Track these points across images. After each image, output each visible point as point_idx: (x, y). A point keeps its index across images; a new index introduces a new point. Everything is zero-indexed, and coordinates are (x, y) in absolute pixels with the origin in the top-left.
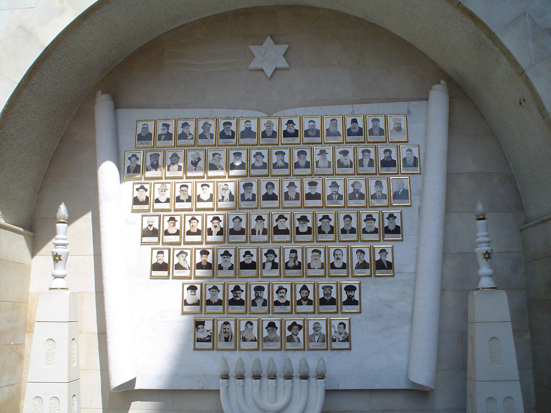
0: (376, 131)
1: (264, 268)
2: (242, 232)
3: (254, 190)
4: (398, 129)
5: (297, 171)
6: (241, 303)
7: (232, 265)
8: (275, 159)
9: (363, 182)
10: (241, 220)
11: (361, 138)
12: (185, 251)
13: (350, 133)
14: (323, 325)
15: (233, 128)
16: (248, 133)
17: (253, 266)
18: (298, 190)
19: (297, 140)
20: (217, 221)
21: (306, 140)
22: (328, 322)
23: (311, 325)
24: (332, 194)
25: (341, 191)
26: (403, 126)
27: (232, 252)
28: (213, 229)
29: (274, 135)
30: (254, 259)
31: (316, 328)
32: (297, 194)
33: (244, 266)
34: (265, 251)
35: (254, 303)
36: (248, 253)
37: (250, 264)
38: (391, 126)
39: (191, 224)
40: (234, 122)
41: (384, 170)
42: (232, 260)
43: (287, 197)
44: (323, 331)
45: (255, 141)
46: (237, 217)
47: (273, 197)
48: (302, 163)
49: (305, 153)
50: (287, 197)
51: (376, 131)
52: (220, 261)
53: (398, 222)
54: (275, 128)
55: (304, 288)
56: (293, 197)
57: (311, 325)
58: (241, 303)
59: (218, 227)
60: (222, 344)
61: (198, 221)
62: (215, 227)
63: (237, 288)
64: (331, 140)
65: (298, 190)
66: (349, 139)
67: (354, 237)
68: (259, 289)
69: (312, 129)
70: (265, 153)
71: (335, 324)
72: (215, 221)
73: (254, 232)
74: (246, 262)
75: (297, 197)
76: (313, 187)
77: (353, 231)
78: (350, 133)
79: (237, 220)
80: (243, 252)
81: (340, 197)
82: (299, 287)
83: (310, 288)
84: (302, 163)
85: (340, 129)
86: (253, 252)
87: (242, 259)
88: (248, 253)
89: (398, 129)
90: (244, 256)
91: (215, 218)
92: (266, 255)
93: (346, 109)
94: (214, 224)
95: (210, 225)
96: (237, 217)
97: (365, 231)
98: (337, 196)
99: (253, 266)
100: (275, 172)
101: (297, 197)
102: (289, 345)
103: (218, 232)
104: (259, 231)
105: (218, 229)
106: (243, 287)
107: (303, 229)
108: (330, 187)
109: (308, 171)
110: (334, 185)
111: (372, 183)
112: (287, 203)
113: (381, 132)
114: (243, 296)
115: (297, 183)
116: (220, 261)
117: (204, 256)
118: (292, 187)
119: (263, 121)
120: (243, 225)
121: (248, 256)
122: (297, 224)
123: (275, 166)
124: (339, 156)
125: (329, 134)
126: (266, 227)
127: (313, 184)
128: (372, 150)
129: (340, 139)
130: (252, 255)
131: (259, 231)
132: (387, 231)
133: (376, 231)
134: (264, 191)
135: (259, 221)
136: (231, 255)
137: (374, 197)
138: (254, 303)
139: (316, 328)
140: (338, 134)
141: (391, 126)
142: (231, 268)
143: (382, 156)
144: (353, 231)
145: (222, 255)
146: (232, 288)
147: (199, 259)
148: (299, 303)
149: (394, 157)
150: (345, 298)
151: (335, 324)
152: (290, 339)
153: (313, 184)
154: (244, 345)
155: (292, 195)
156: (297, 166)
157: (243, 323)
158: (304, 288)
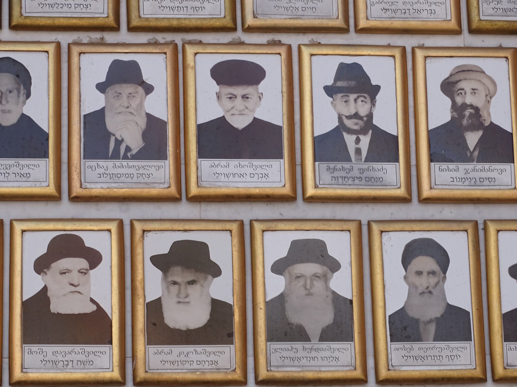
18: (158, 105)
24: (341, 128)
25: (387, 116)
32: (154, 127)
43: (98, 139)
50: (98, 139)
56: (134, 140)
65: (158, 105)
75: (153, 143)
76: (239, 91)
81: (384, 147)
98: (365, 140)
101: (153, 143)
107: (189, 313)
108: (330, 91)
110: (353, 82)
112: (97, 176)
115: (155, 68)
118: (127, 89)
122: (153, 283)
127: (236, 75)
153: (236, 75)
155: (128, 131)
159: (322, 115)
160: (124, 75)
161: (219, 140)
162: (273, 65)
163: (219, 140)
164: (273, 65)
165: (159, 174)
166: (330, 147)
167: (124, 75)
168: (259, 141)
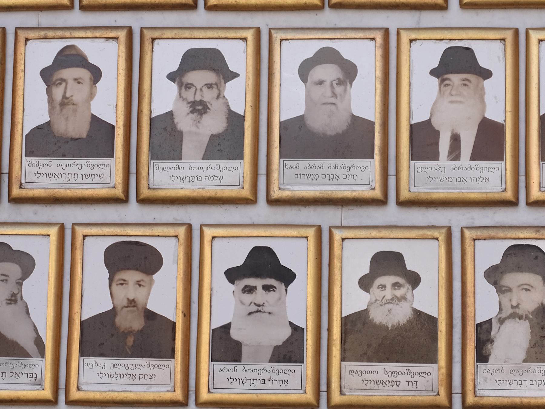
1: (482, 357)
2: (353, 141)
7: (297, 331)
10: (349, 71)
12: (16, 244)
17: (414, 341)
20: (209, 77)
27: (294, 254)
28: (184, 122)
30: (428, 299)
33: (365, 339)
34: (490, 253)
36: (388, 263)
37: (400, 329)
39: (58, 93)
42: (297, 304)
46: (327, 56)
52: (223, 304)
59: (216, 106)
61: (96, 74)
62: (199, 108)
72: (199, 78)
73: (424, 141)
74: (379, 316)
79: (328, 72)
80: (356, 259)
86: (426, 258)
87: (352, 300)
88: (388, 263)
90: (365, 283)
91: (193, 60)
92: (494, 275)
94: (190, 95)
95: (164, 98)
96: (327, 56)
103: (213, 138)
104: (456, 140)
105: (214, 124)
117: (132, 276)
120: (363, 100)
121: (388, 280)
126: (498, 110)
130: (414, 280)
131: (456, 140)
135: (456, 79)
136: (287, 277)
142: (288, 352)
145: (232, 275)
147: (96, 295)
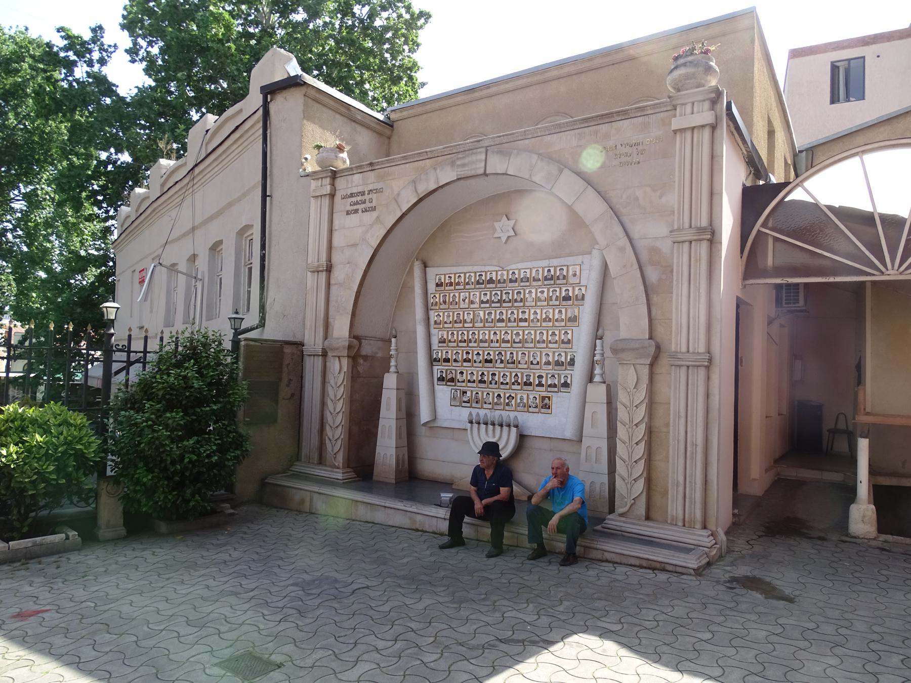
0: (561, 277)
3: (493, 317)
4: (575, 275)
5: (516, 304)
6: (484, 382)
8: (504, 297)
9: (551, 311)
11: (552, 282)
13: (546, 279)
14: (525, 397)
15: (483, 278)
16: (491, 281)
17: (490, 361)
18: (515, 316)
19: (517, 284)
21: (522, 284)
22: (528, 396)
23: (519, 396)
25: (539, 317)
26: (578, 273)
29: (504, 281)
31: (521, 399)
35: (491, 383)
38: (571, 273)
40: (484, 274)
41: (564, 303)
44: (525, 401)
45: (494, 286)
47: (502, 321)
48: (519, 299)
49: (520, 293)
50: (510, 321)
51: (561, 277)
53: (569, 337)
54: (505, 277)
55: (516, 375)
57: (519, 396)
58: (484, 382)
60: (474, 405)
63: (483, 374)
64: (535, 283)
65: (515, 316)
66: (546, 283)
67: (545, 345)
68: (494, 375)
69: (525, 277)
70: (499, 293)
71: (531, 397)
77: (544, 342)
78: (546, 279)
81: (538, 321)
82: (514, 374)
83: (519, 375)
84: (519, 299)
85: (540, 277)
89: (575, 275)
93: (545, 263)
97: (550, 342)
99: (490, 361)
100: (504, 305)
102: (507, 408)
106: (486, 373)
109: (522, 304)
110: (535, 313)
111: (557, 311)
112: (509, 324)
113: (564, 277)
114: (486, 378)
115: (515, 312)
116: (475, 358)
119: (499, 273)
123: (504, 301)
124: (539, 294)
125: (534, 280)
127: (524, 312)
128: (558, 289)
129: (540, 283)
132: (563, 342)
133: (556, 342)
134: (498, 317)
137: (557, 320)
138: (491, 383)
139: (521, 399)
140: (539, 280)
141: (571, 273)
143: (563, 294)
144: (544, 342)
146: (480, 373)
148: (513, 384)
149: (571, 294)
150: (537, 382)
151: (531, 397)
152: (508, 404)
154: (485, 406)
155: (512, 319)
156: (516, 301)
157: (485, 394)
158: (516, 375)
159: (532, 317)
160: (512, 313)
161: (521, 320)
162: (527, 311)
163: (521, 320)
164: (527, 311)
165: (515, 324)
166: (532, 321)
167: (512, 313)
168: (525, 320)
